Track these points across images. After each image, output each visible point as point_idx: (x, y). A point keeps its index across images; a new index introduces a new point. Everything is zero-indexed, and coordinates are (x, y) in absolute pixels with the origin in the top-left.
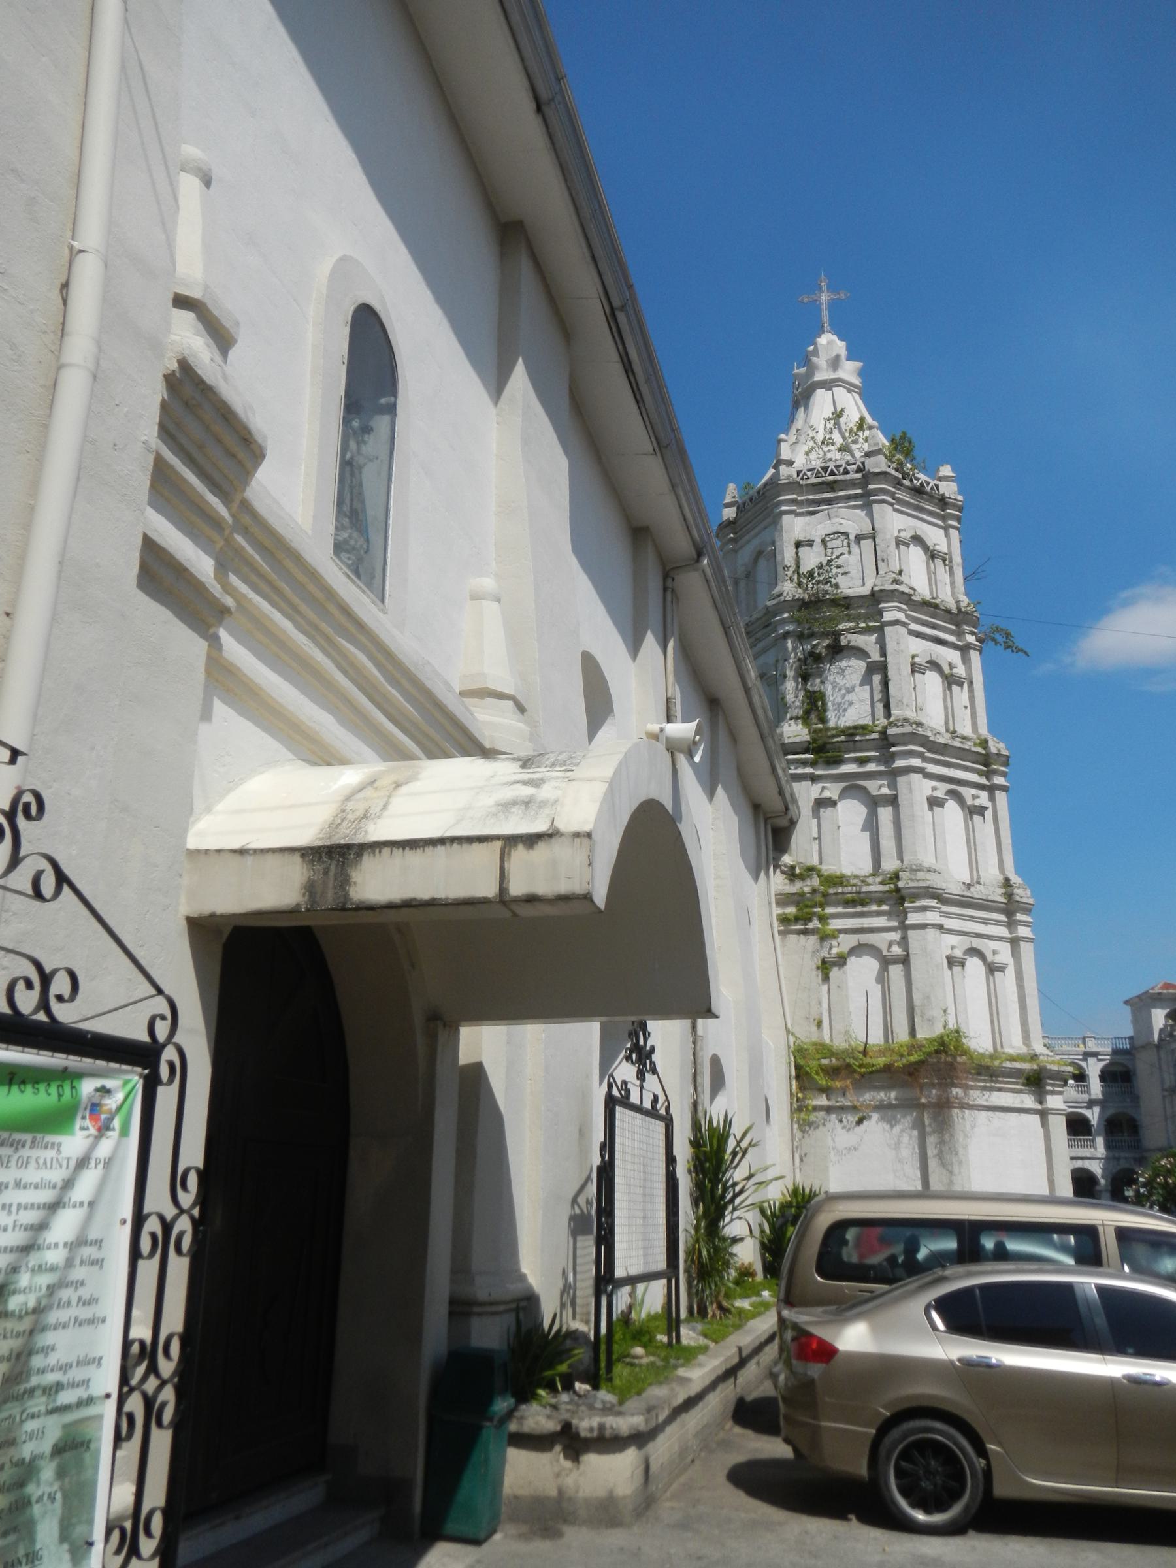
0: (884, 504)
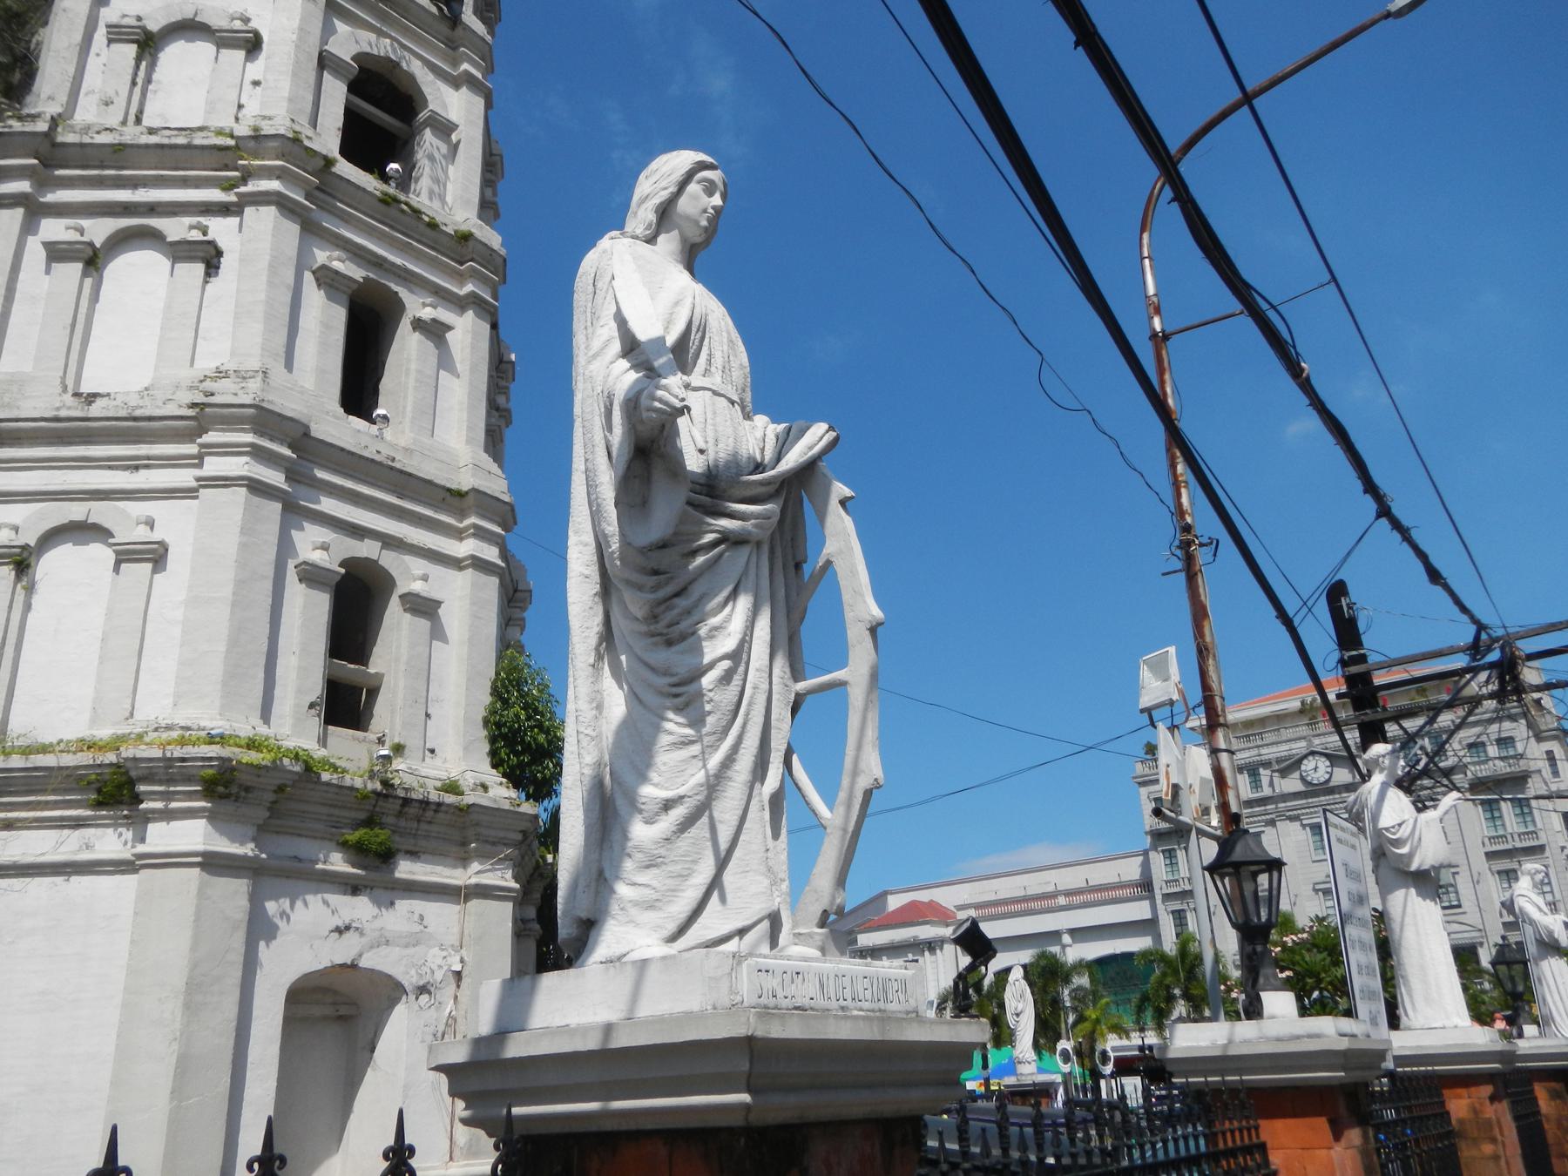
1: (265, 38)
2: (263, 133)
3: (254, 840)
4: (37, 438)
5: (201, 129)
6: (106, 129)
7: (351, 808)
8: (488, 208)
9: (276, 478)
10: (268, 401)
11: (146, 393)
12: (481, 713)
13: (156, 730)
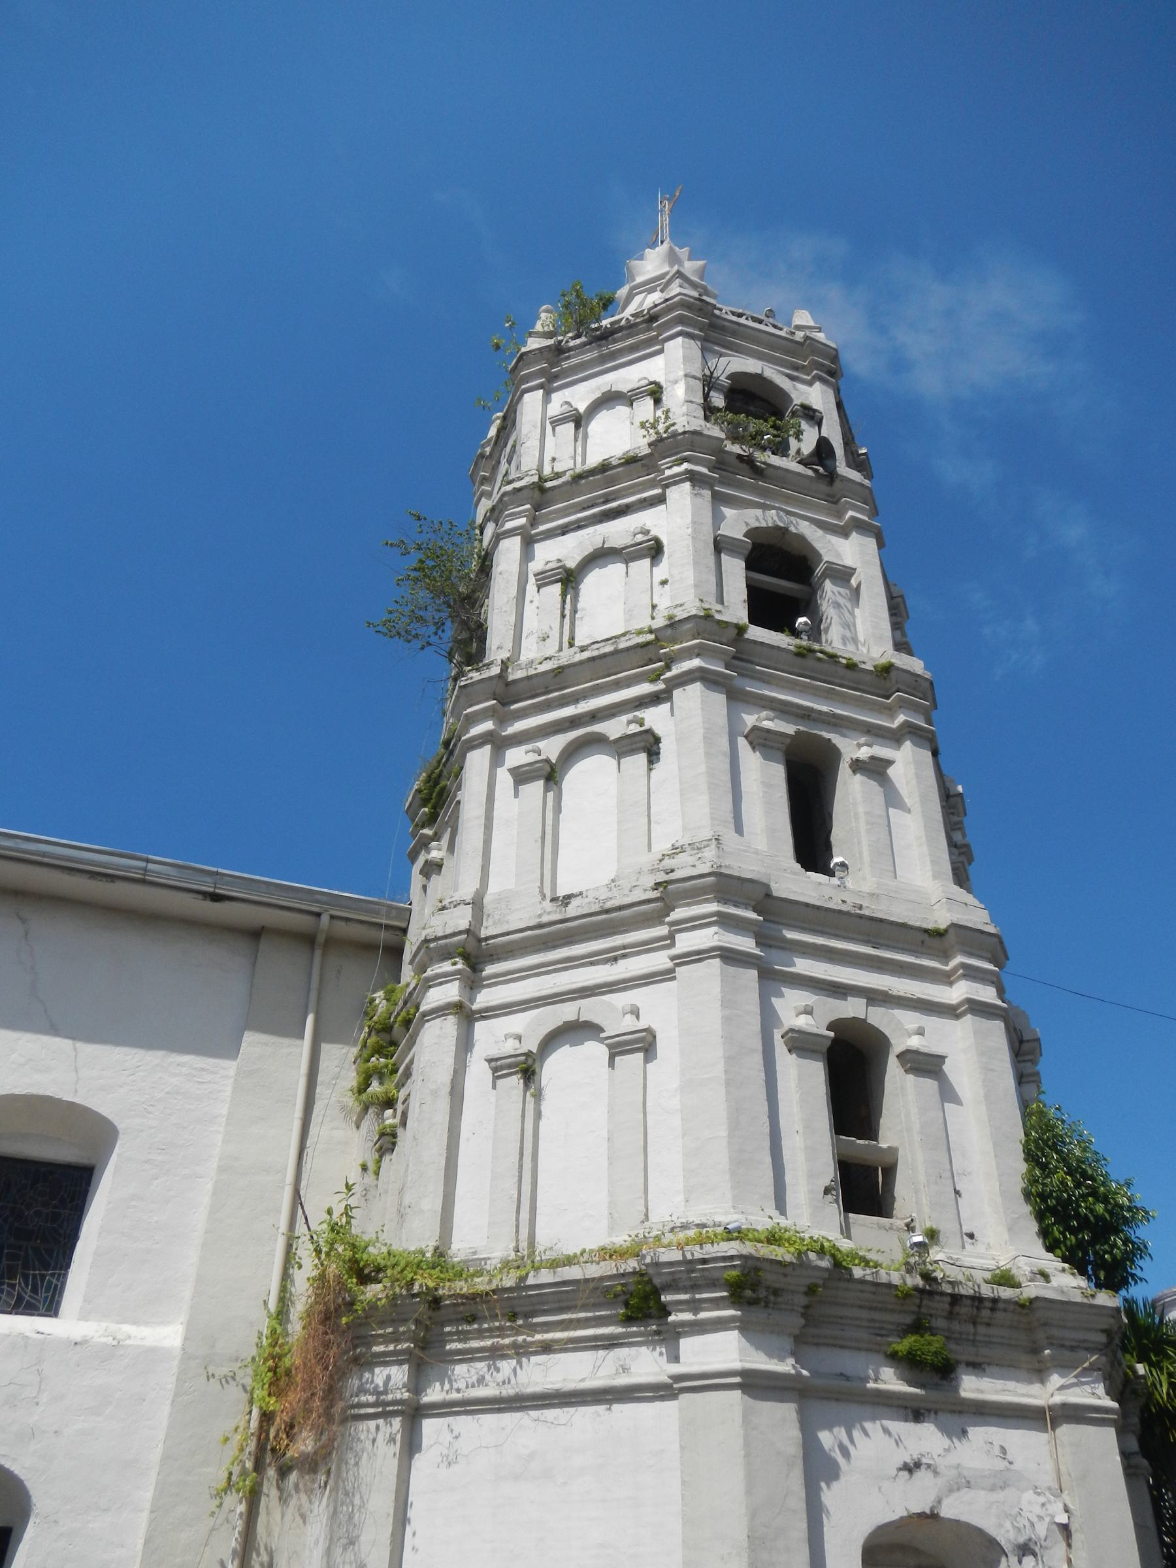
0: (525, 395)
1: (665, 541)
2: (677, 619)
3: (793, 1354)
4: (526, 948)
5: (624, 635)
6: (546, 659)
7: (893, 1311)
8: (901, 646)
9: (746, 944)
10: (726, 866)
11: (613, 884)
12: (1017, 1185)
13: (672, 1230)
